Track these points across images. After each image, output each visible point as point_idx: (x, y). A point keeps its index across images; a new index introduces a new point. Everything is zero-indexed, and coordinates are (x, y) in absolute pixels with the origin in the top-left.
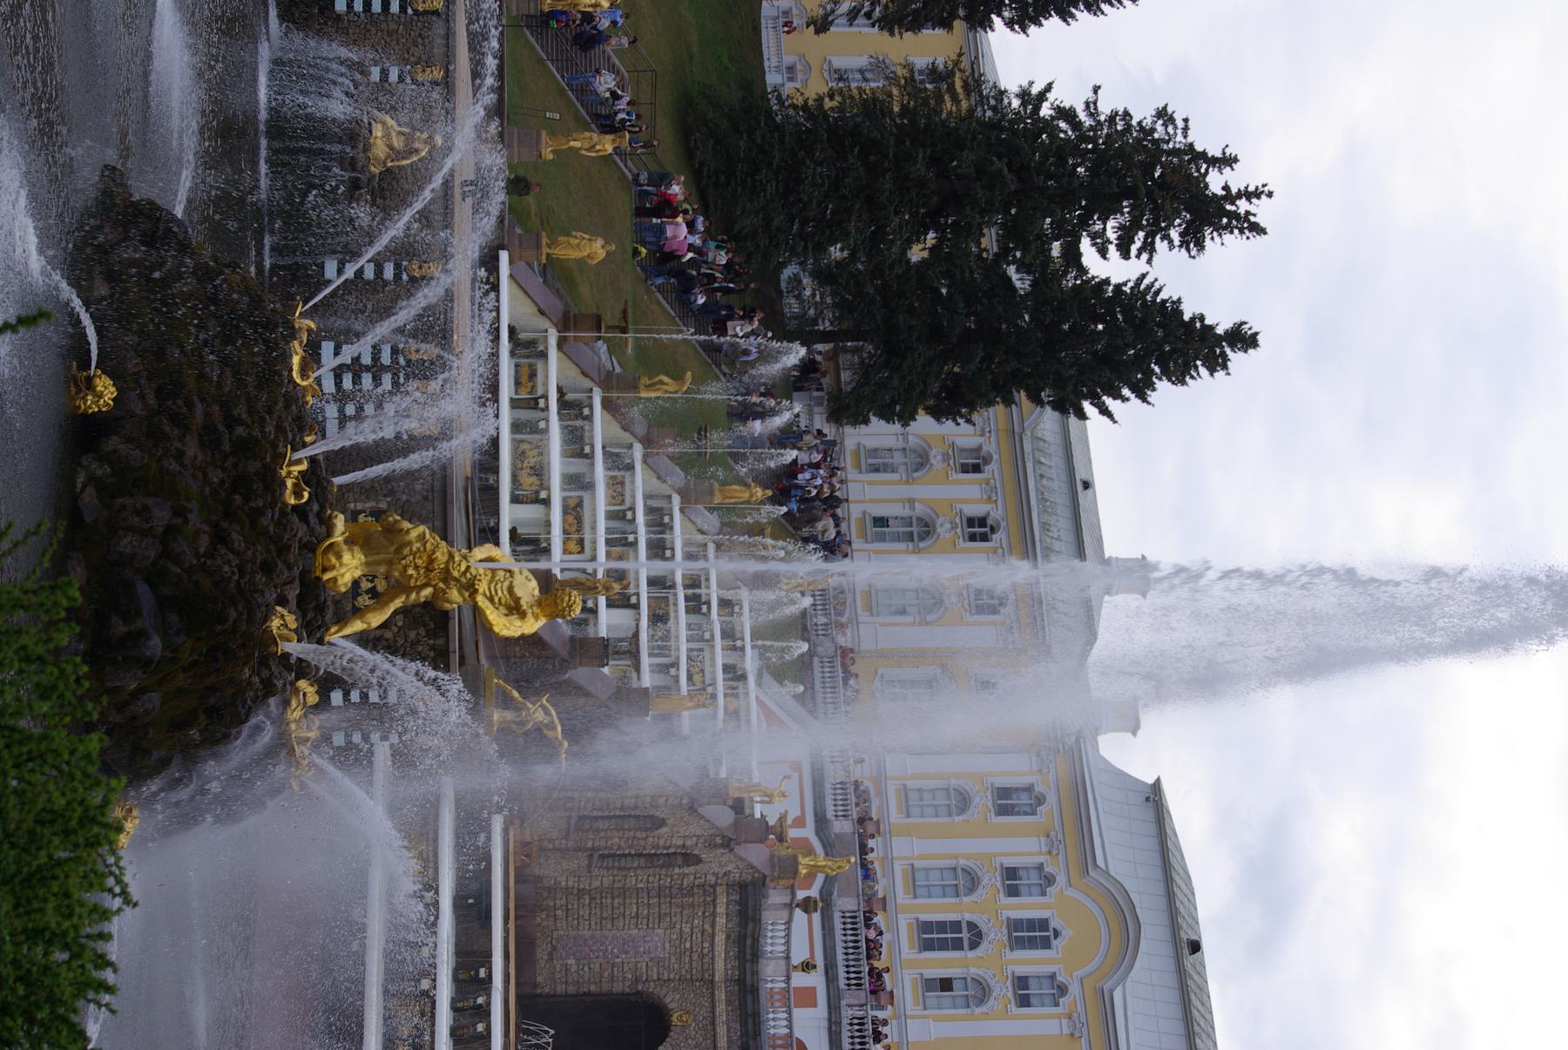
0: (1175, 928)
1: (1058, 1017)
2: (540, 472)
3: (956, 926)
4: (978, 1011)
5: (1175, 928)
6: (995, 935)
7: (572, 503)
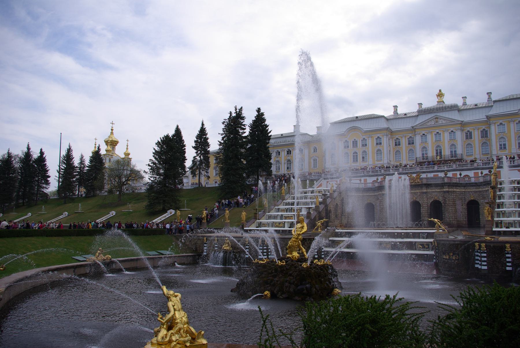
0: (354, 121)
2: (280, 223)
3: (354, 156)
5: (354, 121)
6: (355, 150)
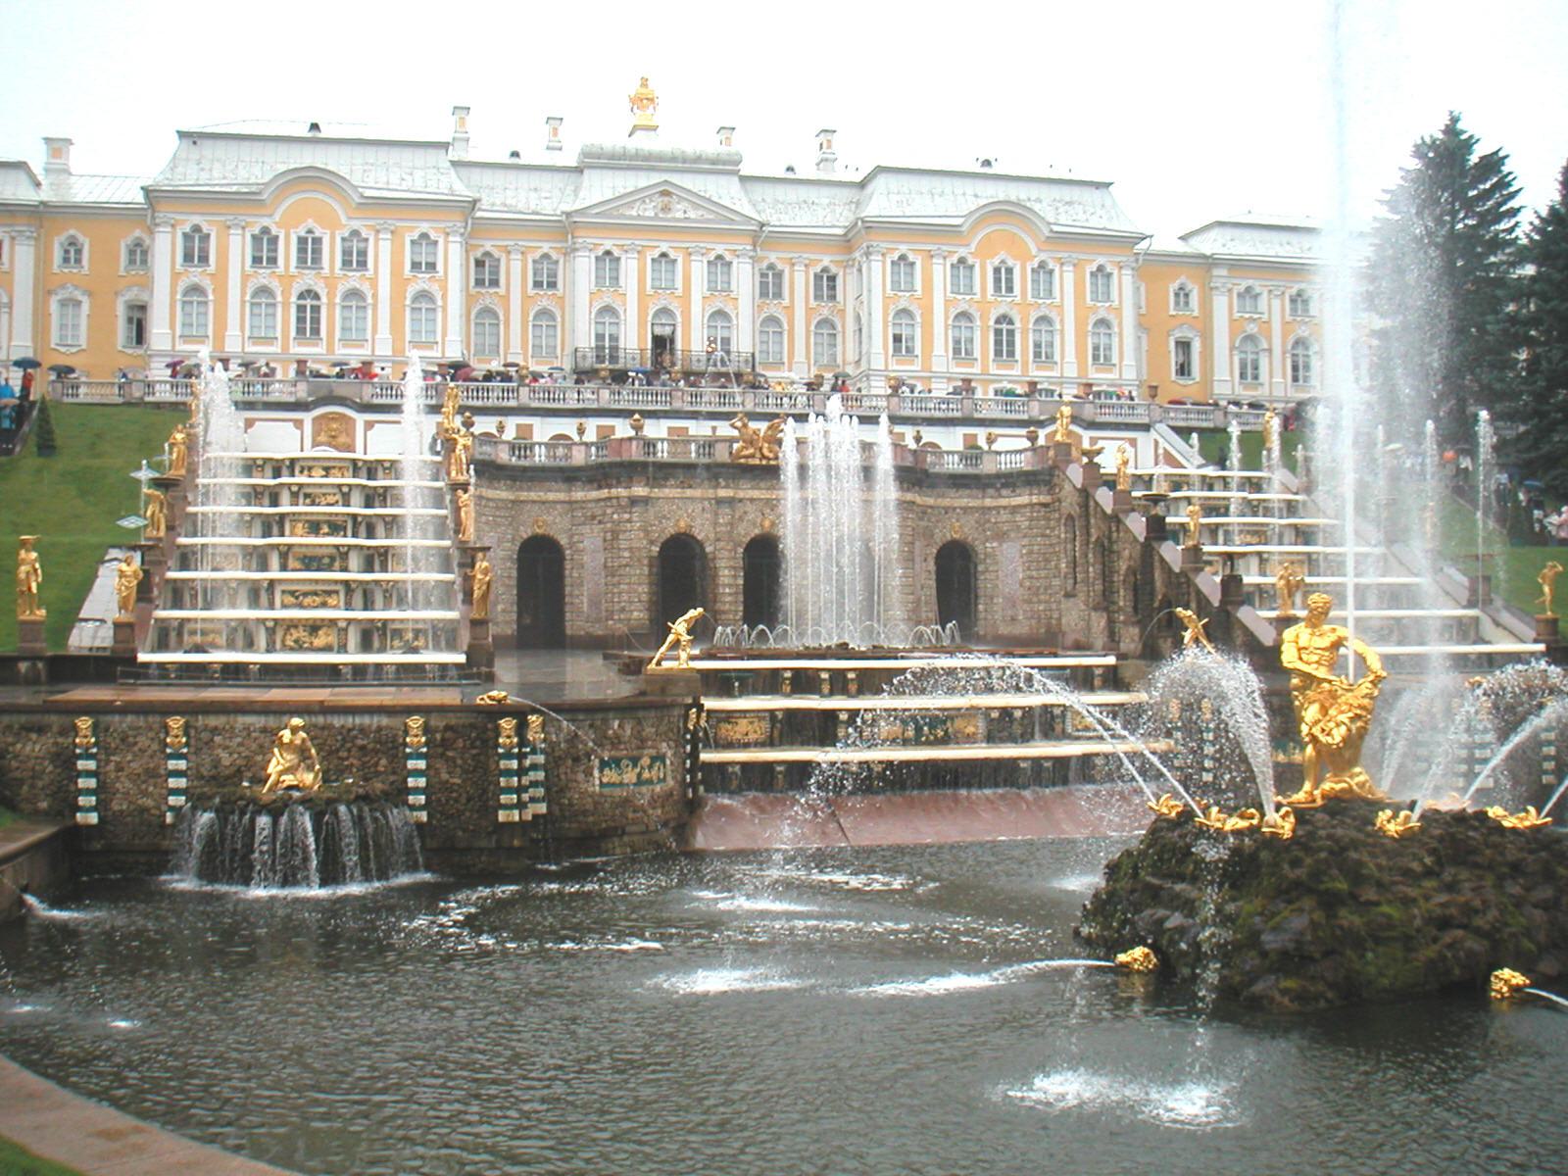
2: (314, 627)
3: (301, 309)
4: (370, 300)
6: (309, 279)
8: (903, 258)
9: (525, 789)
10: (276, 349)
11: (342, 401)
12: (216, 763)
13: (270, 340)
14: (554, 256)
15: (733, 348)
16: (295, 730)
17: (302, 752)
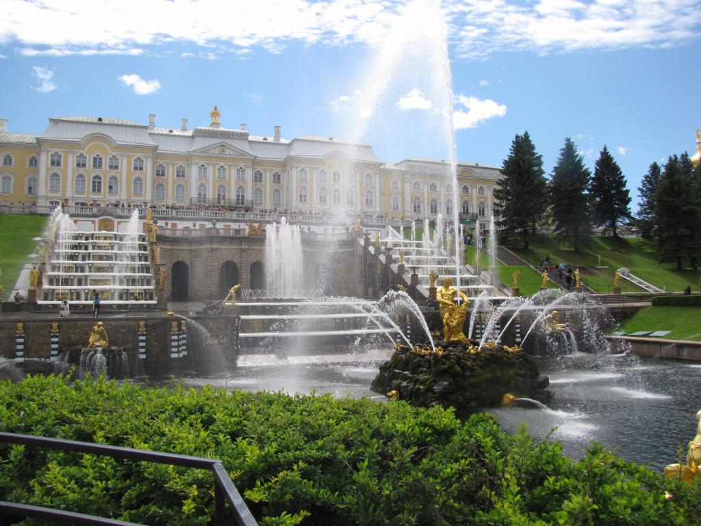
1: (122, 159)
3: (94, 182)
4: (119, 180)
5: (91, 123)
6: (97, 172)
7: (93, 282)
8: (303, 169)
9: (180, 346)
10: (85, 196)
11: (110, 214)
12: (69, 339)
13: (83, 193)
14: (184, 166)
15: (245, 198)
16: (99, 326)
17: (101, 334)
